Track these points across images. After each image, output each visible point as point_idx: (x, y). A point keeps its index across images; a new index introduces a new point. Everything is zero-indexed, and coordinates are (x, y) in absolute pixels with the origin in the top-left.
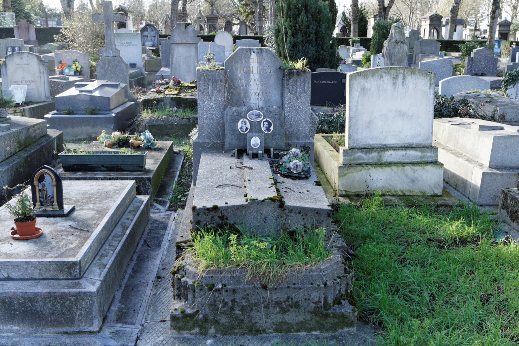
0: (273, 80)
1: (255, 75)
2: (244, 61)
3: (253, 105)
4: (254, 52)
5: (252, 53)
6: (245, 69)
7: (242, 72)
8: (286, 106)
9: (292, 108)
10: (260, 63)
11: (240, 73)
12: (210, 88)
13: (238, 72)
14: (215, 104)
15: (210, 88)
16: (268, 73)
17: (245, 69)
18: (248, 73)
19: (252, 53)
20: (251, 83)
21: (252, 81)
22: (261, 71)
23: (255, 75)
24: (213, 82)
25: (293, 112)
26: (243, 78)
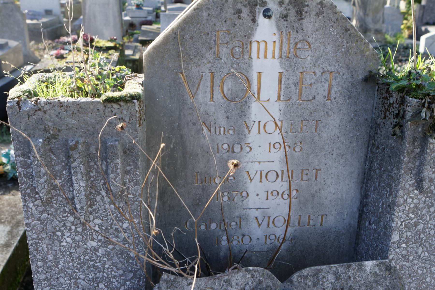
0: (335, 126)
1: (266, 108)
2: (224, 51)
3: (257, 213)
4: (267, 14)
5: (261, 19)
6: (228, 85)
7: (218, 96)
8: (395, 237)
9: (420, 242)
10: (289, 58)
11: (207, 100)
12: (80, 184)
13: (200, 96)
14: (107, 242)
15: (80, 184)
16: (320, 99)
17: (228, 85)
18: (239, 103)
19: (261, 19)
20: (253, 137)
21: (255, 129)
22: (292, 88)
23: (266, 108)
24: (89, 157)
25: (418, 257)
26: (222, 121)
